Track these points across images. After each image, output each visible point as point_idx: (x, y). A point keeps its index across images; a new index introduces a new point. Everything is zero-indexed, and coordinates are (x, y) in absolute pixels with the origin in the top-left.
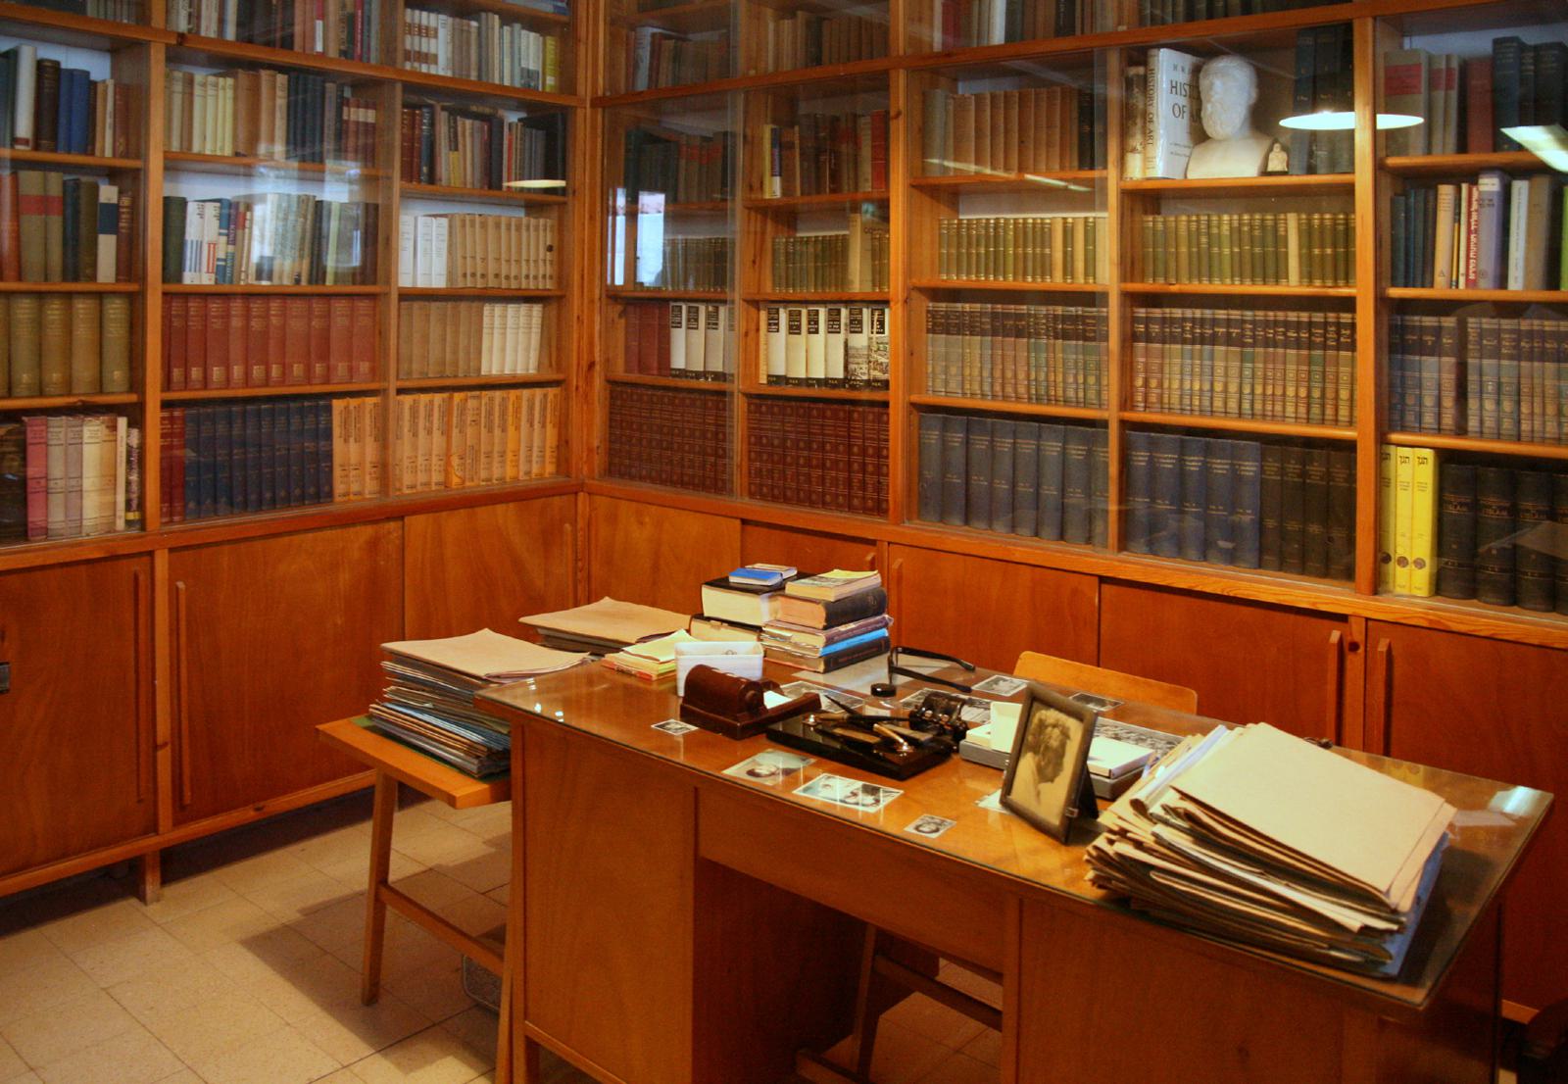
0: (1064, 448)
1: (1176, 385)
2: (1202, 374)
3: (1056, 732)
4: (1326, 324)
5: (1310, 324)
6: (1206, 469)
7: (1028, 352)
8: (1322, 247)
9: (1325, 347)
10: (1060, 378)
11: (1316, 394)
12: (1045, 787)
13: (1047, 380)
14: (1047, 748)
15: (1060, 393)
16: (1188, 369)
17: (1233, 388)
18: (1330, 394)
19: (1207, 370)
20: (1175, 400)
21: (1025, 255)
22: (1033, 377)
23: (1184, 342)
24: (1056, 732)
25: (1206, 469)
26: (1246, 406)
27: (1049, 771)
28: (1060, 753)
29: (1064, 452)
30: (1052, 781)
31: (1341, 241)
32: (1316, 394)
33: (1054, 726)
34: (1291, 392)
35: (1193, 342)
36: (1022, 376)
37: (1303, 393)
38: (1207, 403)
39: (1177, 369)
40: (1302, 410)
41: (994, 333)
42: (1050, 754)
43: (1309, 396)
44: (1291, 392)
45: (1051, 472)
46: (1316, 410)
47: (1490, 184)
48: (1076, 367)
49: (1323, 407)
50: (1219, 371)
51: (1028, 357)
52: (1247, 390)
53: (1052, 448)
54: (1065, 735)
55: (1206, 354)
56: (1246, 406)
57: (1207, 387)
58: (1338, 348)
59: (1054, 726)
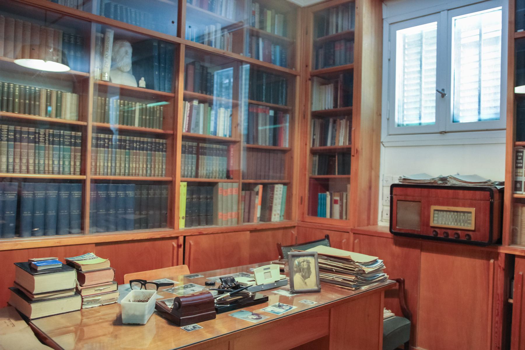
0: (58, 194)
1: (102, 164)
2: (111, 160)
3: (305, 263)
4: (151, 143)
5: (147, 143)
6: (117, 196)
7: (35, 150)
8: (146, 116)
9: (151, 150)
10: (51, 162)
11: (149, 166)
12: (306, 280)
13: (44, 163)
14: (303, 269)
15: (51, 169)
16: (106, 158)
17: (123, 165)
18: (153, 166)
19: (114, 158)
20: (102, 170)
21: (25, 103)
22: (37, 162)
23: (104, 147)
24: (305, 263)
25: (117, 196)
26: (127, 171)
27: (307, 275)
28: (309, 268)
29: (58, 196)
30: (309, 277)
31: (151, 114)
32: (149, 166)
33: (303, 262)
34: (141, 166)
35: (108, 147)
36: (31, 161)
37: (145, 166)
38: (113, 170)
39: (102, 158)
40: (145, 172)
41: (15, 140)
42: (306, 270)
43: (147, 167)
44: (141, 166)
45: (52, 205)
46: (149, 172)
47: (195, 103)
48: (70, 158)
49: (151, 171)
50: (118, 159)
51: (35, 152)
52: (127, 165)
53: (52, 194)
54: (308, 262)
55: (114, 153)
56: (127, 171)
57: (113, 165)
58: (155, 151)
59: (303, 262)
